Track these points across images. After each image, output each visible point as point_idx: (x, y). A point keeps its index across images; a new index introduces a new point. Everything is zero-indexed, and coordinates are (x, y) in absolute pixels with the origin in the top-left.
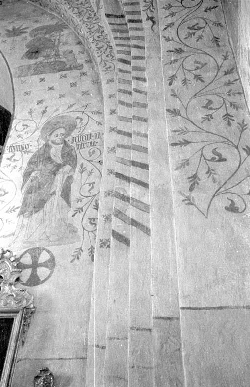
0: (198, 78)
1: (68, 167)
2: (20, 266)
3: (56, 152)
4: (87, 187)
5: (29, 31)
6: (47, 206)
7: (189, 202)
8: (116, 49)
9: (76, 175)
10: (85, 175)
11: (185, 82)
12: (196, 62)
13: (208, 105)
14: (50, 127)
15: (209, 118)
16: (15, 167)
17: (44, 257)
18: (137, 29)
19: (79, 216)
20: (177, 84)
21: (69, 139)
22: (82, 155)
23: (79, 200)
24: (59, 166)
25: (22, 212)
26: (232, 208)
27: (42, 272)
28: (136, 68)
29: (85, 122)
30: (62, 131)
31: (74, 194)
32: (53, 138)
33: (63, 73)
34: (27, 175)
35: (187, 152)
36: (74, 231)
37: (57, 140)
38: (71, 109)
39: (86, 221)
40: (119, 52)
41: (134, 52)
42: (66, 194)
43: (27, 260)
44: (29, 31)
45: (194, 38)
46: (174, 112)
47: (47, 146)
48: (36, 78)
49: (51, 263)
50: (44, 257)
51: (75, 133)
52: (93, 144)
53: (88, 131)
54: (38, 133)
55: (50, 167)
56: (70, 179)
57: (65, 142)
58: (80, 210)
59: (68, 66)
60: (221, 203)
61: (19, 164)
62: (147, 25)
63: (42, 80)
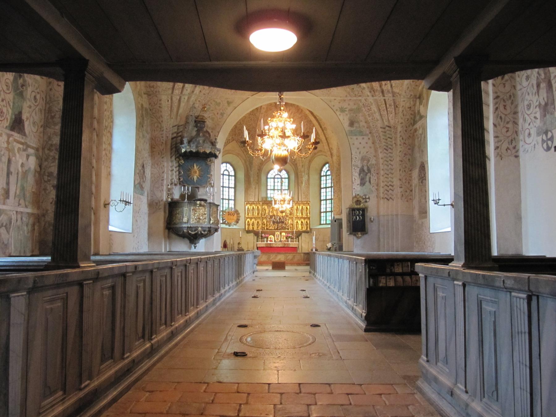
0: (405, 171)
1: (369, 174)
2: (364, 199)
3: (365, 168)
4: (374, 180)
5: (347, 110)
6: (366, 184)
7: (402, 199)
8: (382, 137)
9: (371, 176)
10: (373, 177)
11: (402, 171)
12: (405, 166)
13: (406, 179)
14: (363, 159)
15: (406, 182)
16: (356, 172)
17: (367, 197)
18: (390, 142)
19: (373, 188)
20: (401, 171)
21: (368, 165)
22: (372, 170)
23: (373, 184)
24: (367, 173)
25: (360, 185)
26: (407, 201)
27: (368, 200)
28: (390, 156)
29: (372, 159)
30: (365, 162)
31: (372, 182)
32: (364, 163)
33: (363, 137)
34: (360, 175)
35: (402, 189)
36: (372, 191)
37: (366, 164)
38: (367, 154)
39: (375, 189)
40: (385, 145)
41: (390, 150)
42: (370, 182)
43: (364, 197)
44: (347, 110)
45: (405, 158)
46: (400, 180)
47: (363, 166)
48: (355, 137)
49: (369, 198)
50: (367, 197)
51: (370, 163)
52: (375, 167)
53: (373, 163)
54: (360, 161)
55: (365, 173)
56: (370, 178)
57: (368, 166)
58: (373, 186)
59: (364, 134)
60: (406, 200)
61: (357, 171)
62: (394, 145)
63: (357, 139)
